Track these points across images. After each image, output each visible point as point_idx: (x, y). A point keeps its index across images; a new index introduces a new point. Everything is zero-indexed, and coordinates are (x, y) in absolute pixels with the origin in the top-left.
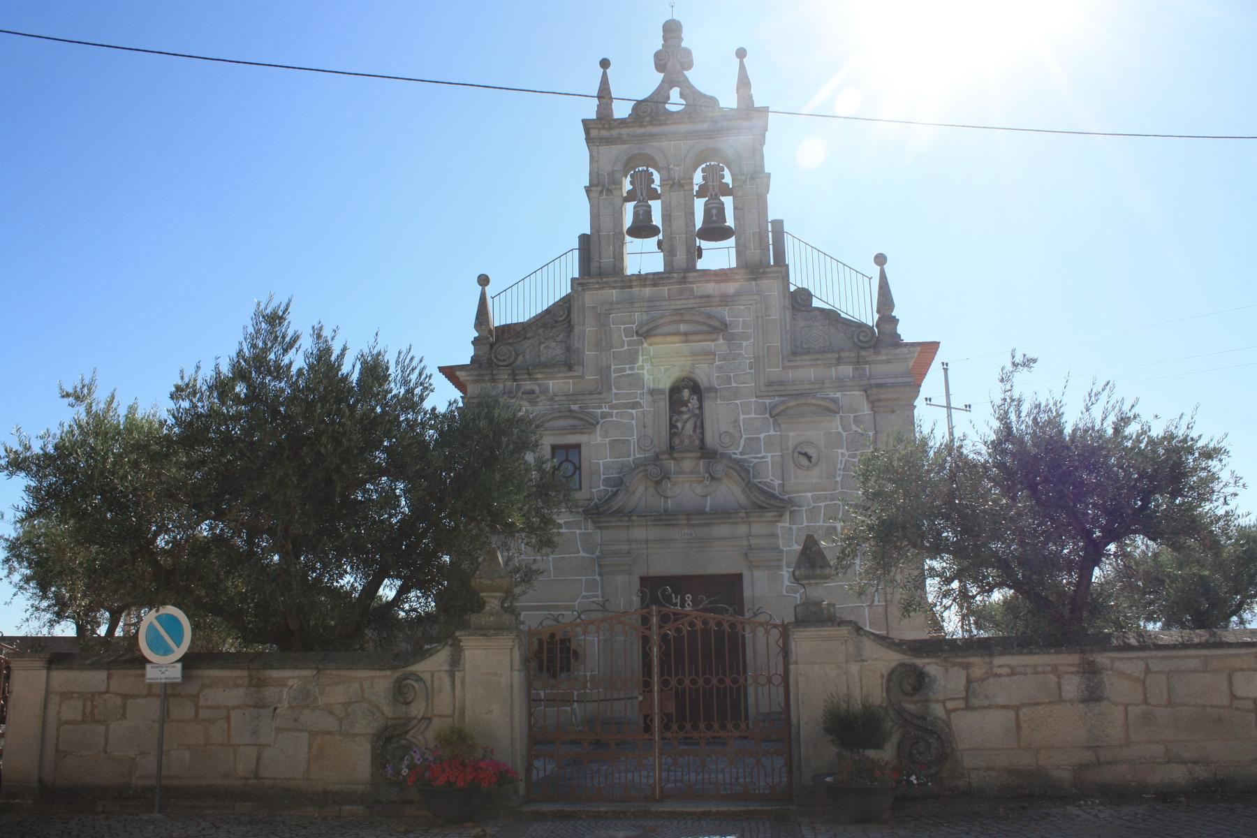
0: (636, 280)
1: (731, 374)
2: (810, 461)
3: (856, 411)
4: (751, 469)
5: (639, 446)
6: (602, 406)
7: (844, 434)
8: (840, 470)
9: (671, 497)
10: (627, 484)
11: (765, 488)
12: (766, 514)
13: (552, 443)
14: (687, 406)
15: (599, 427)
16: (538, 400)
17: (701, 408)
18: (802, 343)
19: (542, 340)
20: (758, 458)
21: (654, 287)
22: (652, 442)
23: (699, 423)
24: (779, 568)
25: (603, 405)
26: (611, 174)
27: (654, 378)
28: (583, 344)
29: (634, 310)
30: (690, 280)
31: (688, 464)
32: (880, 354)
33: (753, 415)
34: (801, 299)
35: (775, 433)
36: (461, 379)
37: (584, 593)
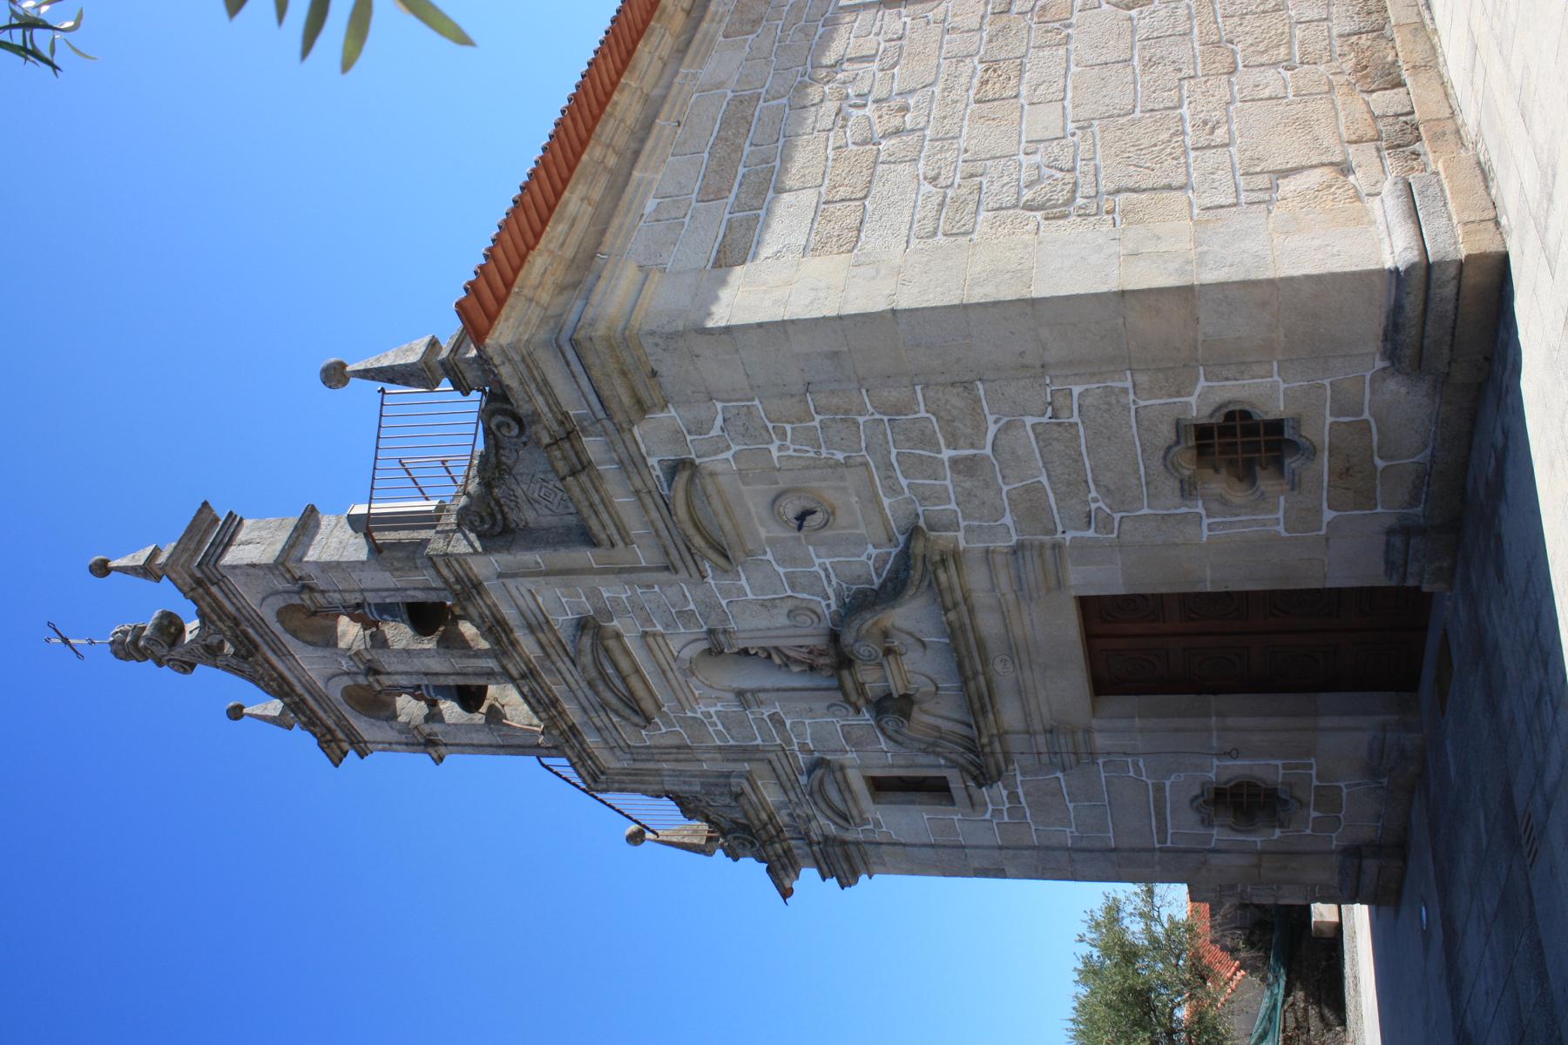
0: (558, 728)
3: (678, 432)
4: (854, 587)
7: (735, 448)
11: (888, 567)
20: (828, 576)
21: (557, 700)
24: (1057, 547)
30: (525, 668)
37: (1132, 774)
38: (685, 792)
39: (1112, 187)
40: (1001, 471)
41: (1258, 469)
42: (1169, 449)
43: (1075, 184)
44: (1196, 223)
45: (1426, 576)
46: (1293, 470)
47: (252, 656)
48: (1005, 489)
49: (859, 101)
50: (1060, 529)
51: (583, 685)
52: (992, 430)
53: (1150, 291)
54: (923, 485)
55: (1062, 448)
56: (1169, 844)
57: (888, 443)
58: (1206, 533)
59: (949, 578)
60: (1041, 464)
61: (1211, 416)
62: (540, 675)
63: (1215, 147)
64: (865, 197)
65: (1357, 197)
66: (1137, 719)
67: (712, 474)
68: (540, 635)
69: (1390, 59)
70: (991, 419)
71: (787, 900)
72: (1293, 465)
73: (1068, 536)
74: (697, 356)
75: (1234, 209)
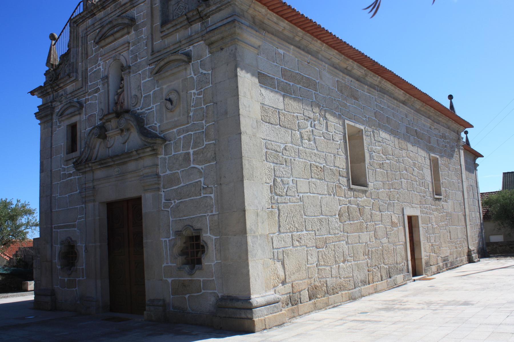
0: (94, 9)
3: (201, 57)
4: (145, 119)
7: (195, 77)
11: (152, 131)
20: (149, 109)
21: (105, 9)
24: (159, 189)
37: (79, 216)
38: (70, 56)
39: (280, 208)
40: (185, 170)
41: (185, 256)
42: (192, 227)
43: (282, 196)
44: (267, 235)
45: (149, 312)
46: (185, 268)
48: (179, 171)
49: (313, 125)
50: (165, 190)
51: (110, 19)
52: (199, 167)
53: (245, 220)
54: (181, 143)
55: (193, 191)
56: (54, 230)
57: (195, 131)
58: (163, 240)
59: (148, 152)
60: (187, 183)
61: (203, 241)
62: (114, 3)
63: (292, 241)
64: (280, 126)
65: (274, 287)
66: (98, 218)
67: (186, 69)
68: (129, 4)
69: (318, 296)
70: (203, 166)
71: (30, 93)
72: (186, 268)
73: (162, 193)
74: (227, 65)
75: (272, 248)
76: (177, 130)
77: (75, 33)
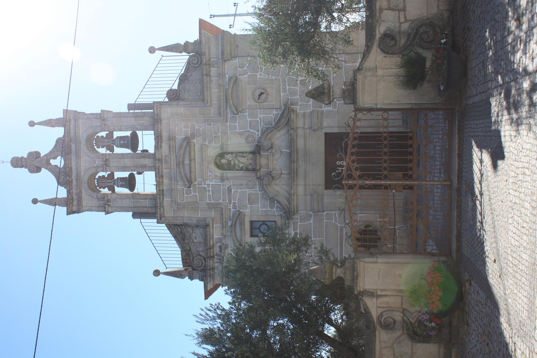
0: (159, 187)
1: (214, 135)
2: (264, 93)
3: (236, 67)
4: (267, 126)
5: (252, 188)
6: (229, 208)
7: (249, 74)
8: (269, 77)
9: (281, 171)
10: (273, 195)
11: (278, 118)
12: (292, 118)
13: (249, 237)
14: (231, 161)
15: (241, 210)
16: (225, 244)
17: (232, 153)
18: (197, 96)
19: (191, 241)
20: (261, 122)
21: (163, 177)
22: (250, 181)
23: (241, 155)
24: (322, 112)
25: (229, 207)
26: (98, 199)
27: (215, 179)
28: (194, 218)
29: (176, 189)
30: (160, 157)
31: (263, 161)
32: (205, 53)
33: (237, 124)
34: (173, 95)
35: (247, 112)
36: (212, 287)
37: (334, 221)
47: (68, 155)
54: (292, 88)
59: (294, 118)
62: (163, 163)
68: (171, 142)
76: (282, 92)
77: (171, 219)
